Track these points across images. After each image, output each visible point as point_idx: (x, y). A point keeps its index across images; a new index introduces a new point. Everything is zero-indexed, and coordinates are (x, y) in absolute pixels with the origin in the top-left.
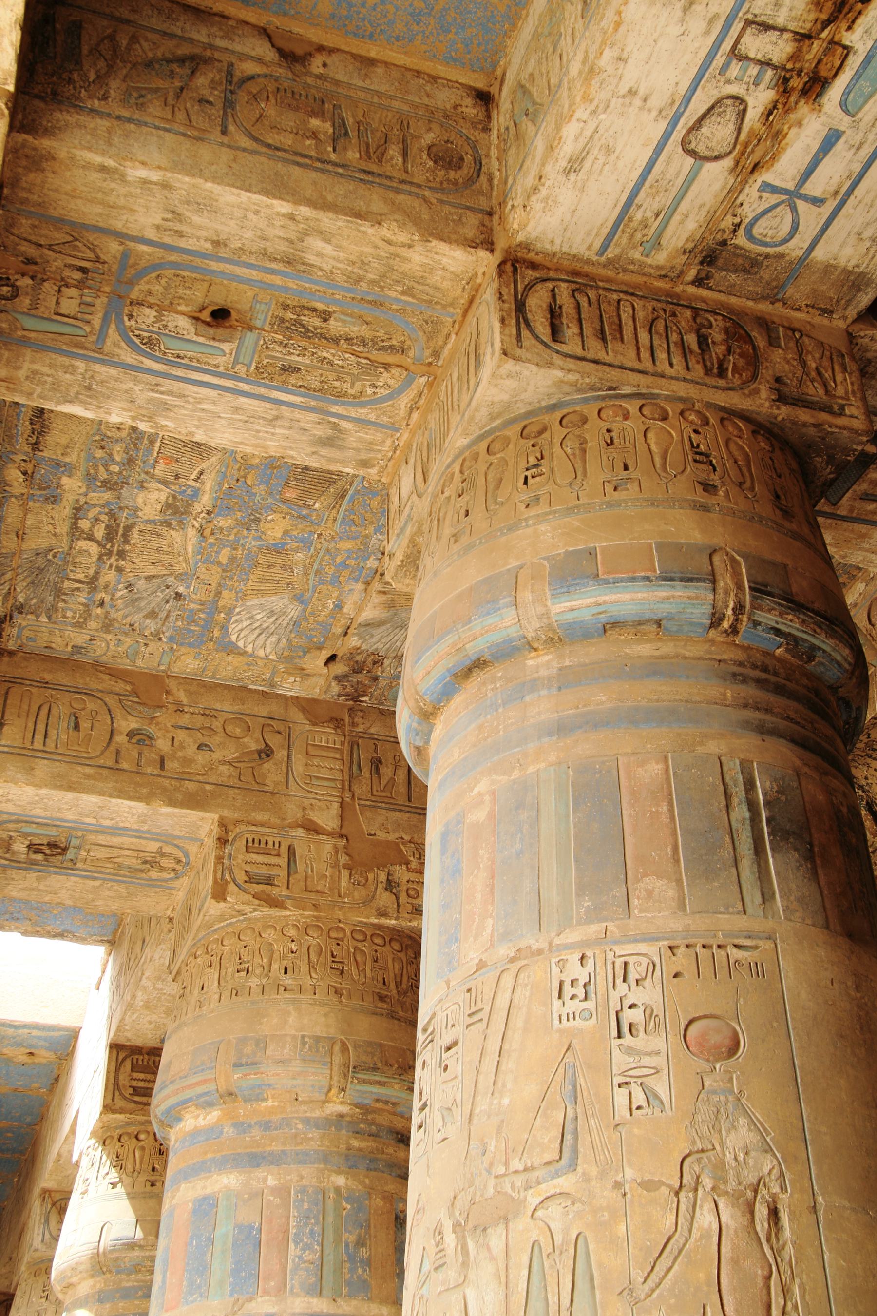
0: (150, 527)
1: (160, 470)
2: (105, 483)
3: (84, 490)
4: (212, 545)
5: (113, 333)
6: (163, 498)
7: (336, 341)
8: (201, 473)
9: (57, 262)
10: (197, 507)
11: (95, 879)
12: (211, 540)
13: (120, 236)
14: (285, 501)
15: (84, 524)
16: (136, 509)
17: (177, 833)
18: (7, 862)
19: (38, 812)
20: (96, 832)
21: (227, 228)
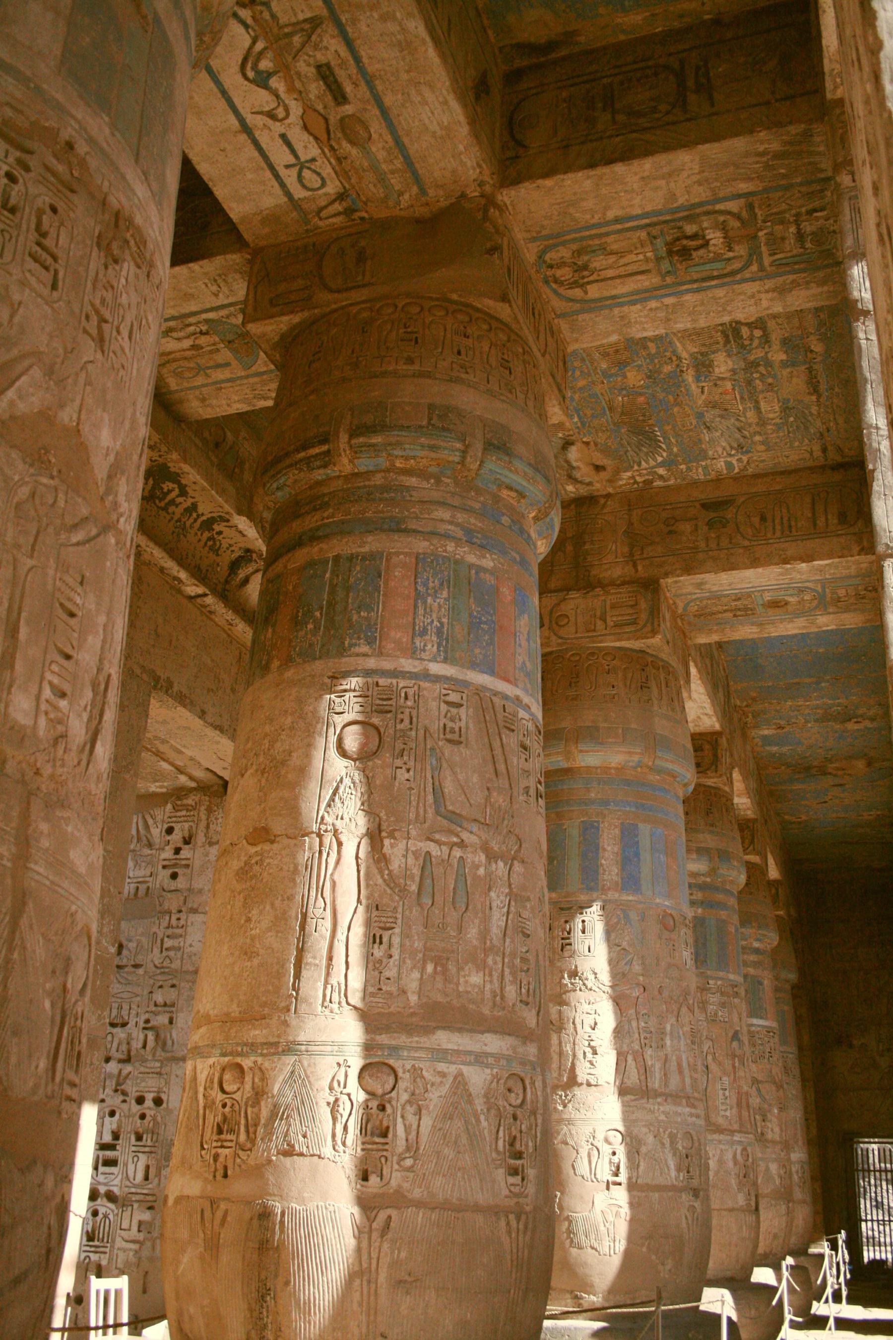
0: (714, 347)
1: (729, 385)
2: (758, 365)
3: (769, 355)
4: (665, 351)
5: (819, 589)
6: (717, 370)
7: (725, 611)
8: (703, 392)
9: (852, 600)
10: (691, 372)
11: (617, 220)
12: (668, 354)
13: (830, 613)
14: (641, 394)
15: (758, 333)
16: (729, 356)
17: (586, 316)
18: (718, 207)
19: (720, 292)
20: (656, 289)
21: (790, 626)
